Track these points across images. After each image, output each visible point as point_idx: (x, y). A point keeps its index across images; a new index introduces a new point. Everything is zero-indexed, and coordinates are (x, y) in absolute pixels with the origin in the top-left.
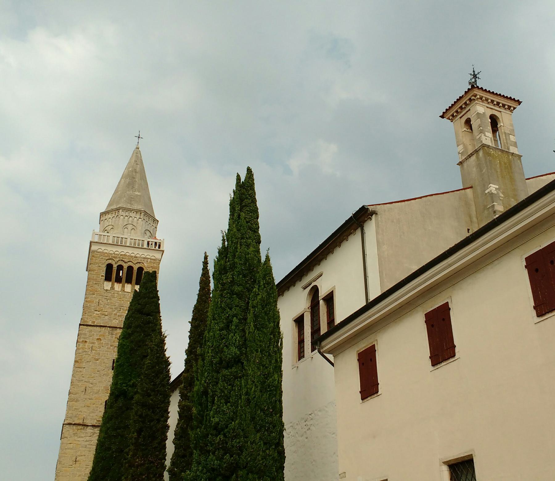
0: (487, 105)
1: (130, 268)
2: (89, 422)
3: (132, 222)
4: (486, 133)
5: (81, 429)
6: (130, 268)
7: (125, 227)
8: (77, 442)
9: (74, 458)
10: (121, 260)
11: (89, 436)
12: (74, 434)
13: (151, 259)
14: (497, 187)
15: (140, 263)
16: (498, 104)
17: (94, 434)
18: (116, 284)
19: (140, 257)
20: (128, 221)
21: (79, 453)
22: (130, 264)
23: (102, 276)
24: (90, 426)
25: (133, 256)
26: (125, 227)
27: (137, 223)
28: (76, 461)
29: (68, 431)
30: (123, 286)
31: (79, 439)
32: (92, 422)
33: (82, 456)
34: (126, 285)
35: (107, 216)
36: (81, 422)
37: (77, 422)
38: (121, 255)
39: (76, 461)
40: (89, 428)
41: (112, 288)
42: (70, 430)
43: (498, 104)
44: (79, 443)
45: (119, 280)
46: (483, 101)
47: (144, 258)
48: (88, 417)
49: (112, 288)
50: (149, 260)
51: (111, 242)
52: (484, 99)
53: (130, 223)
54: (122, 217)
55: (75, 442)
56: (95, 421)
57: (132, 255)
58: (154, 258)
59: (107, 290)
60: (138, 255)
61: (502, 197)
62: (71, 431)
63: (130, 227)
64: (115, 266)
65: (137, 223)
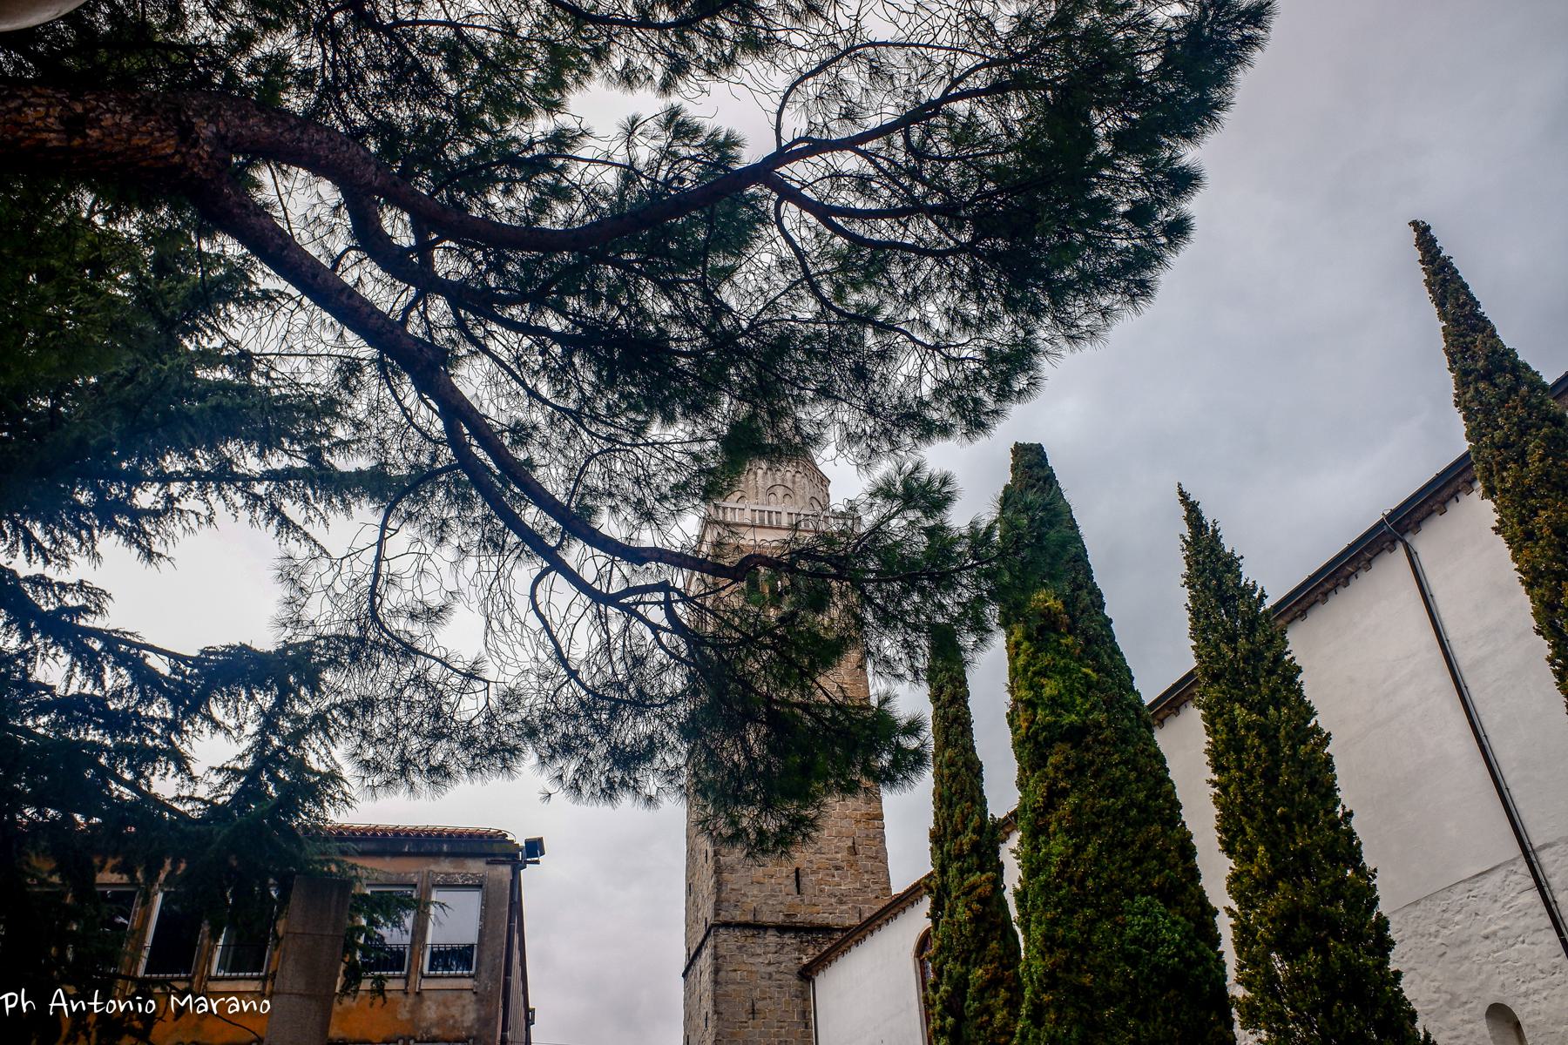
2: (766, 918)
3: (783, 480)
5: (753, 936)
7: (770, 491)
8: (750, 968)
9: (748, 1005)
11: (774, 950)
12: (740, 948)
17: (782, 947)
20: (774, 479)
21: (757, 994)
24: (772, 927)
26: (770, 491)
27: (794, 482)
28: (753, 1012)
29: (725, 941)
31: (751, 960)
32: (774, 919)
33: (764, 999)
36: (749, 918)
37: (743, 919)
39: (753, 1012)
40: (770, 932)
42: (729, 941)
44: (754, 969)
48: (765, 908)
53: (779, 482)
55: (744, 967)
56: (781, 917)
62: (731, 941)
63: (780, 491)
65: (794, 482)
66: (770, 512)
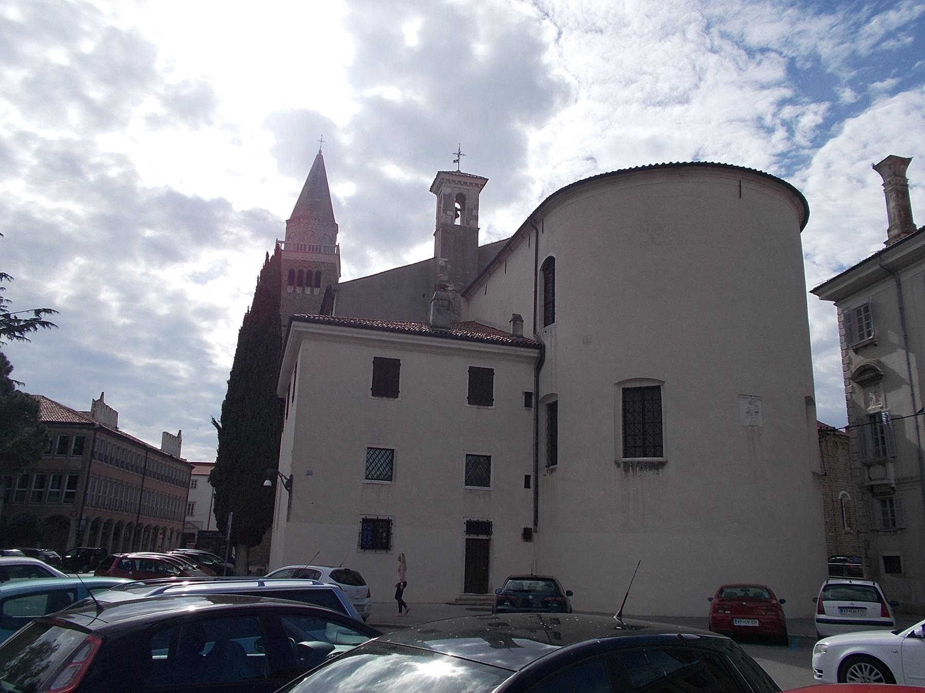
0: (455, 186)
1: (310, 273)
4: (448, 212)
6: (310, 273)
10: (302, 265)
13: (328, 263)
14: (447, 260)
15: (318, 267)
16: (465, 183)
18: (297, 287)
19: (318, 262)
22: (310, 268)
23: (286, 281)
25: (311, 262)
30: (304, 290)
34: (306, 288)
35: (291, 224)
38: (301, 261)
41: (294, 291)
43: (465, 183)
45: (300, 284)
46: (450, 183)
47: (322, 263)
49: (294, 291)
50: (326, 264)
51: (292, 249)
52: (451, 181)
53: (310, 229)
54: (302, 225)
57: (311, 260)
58: (331, 262)
59: (290, 293)
60: (315, 260)
61: (449, 268)
64: (296, 271)
66: (302, 245)
